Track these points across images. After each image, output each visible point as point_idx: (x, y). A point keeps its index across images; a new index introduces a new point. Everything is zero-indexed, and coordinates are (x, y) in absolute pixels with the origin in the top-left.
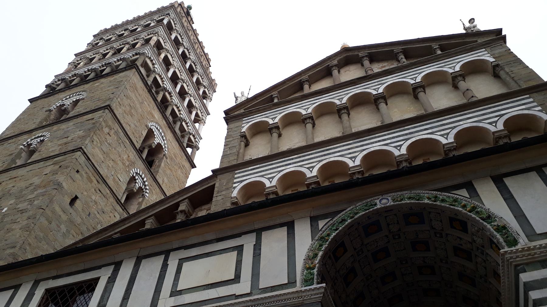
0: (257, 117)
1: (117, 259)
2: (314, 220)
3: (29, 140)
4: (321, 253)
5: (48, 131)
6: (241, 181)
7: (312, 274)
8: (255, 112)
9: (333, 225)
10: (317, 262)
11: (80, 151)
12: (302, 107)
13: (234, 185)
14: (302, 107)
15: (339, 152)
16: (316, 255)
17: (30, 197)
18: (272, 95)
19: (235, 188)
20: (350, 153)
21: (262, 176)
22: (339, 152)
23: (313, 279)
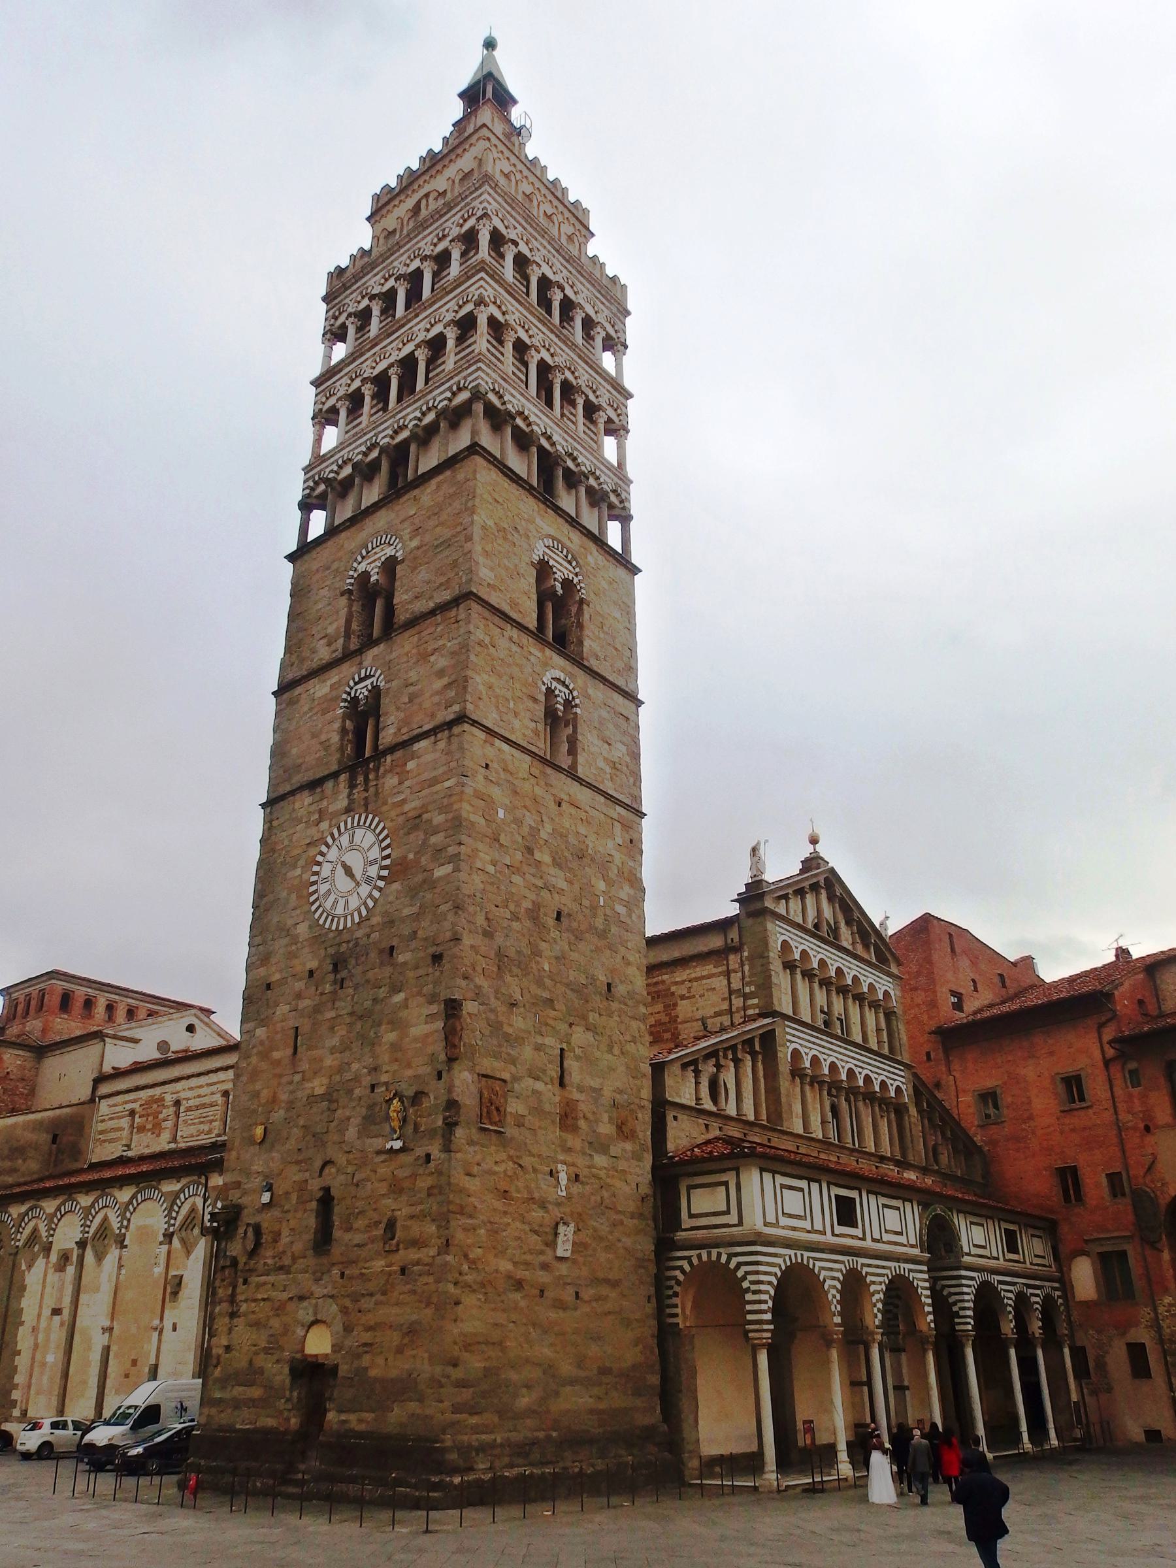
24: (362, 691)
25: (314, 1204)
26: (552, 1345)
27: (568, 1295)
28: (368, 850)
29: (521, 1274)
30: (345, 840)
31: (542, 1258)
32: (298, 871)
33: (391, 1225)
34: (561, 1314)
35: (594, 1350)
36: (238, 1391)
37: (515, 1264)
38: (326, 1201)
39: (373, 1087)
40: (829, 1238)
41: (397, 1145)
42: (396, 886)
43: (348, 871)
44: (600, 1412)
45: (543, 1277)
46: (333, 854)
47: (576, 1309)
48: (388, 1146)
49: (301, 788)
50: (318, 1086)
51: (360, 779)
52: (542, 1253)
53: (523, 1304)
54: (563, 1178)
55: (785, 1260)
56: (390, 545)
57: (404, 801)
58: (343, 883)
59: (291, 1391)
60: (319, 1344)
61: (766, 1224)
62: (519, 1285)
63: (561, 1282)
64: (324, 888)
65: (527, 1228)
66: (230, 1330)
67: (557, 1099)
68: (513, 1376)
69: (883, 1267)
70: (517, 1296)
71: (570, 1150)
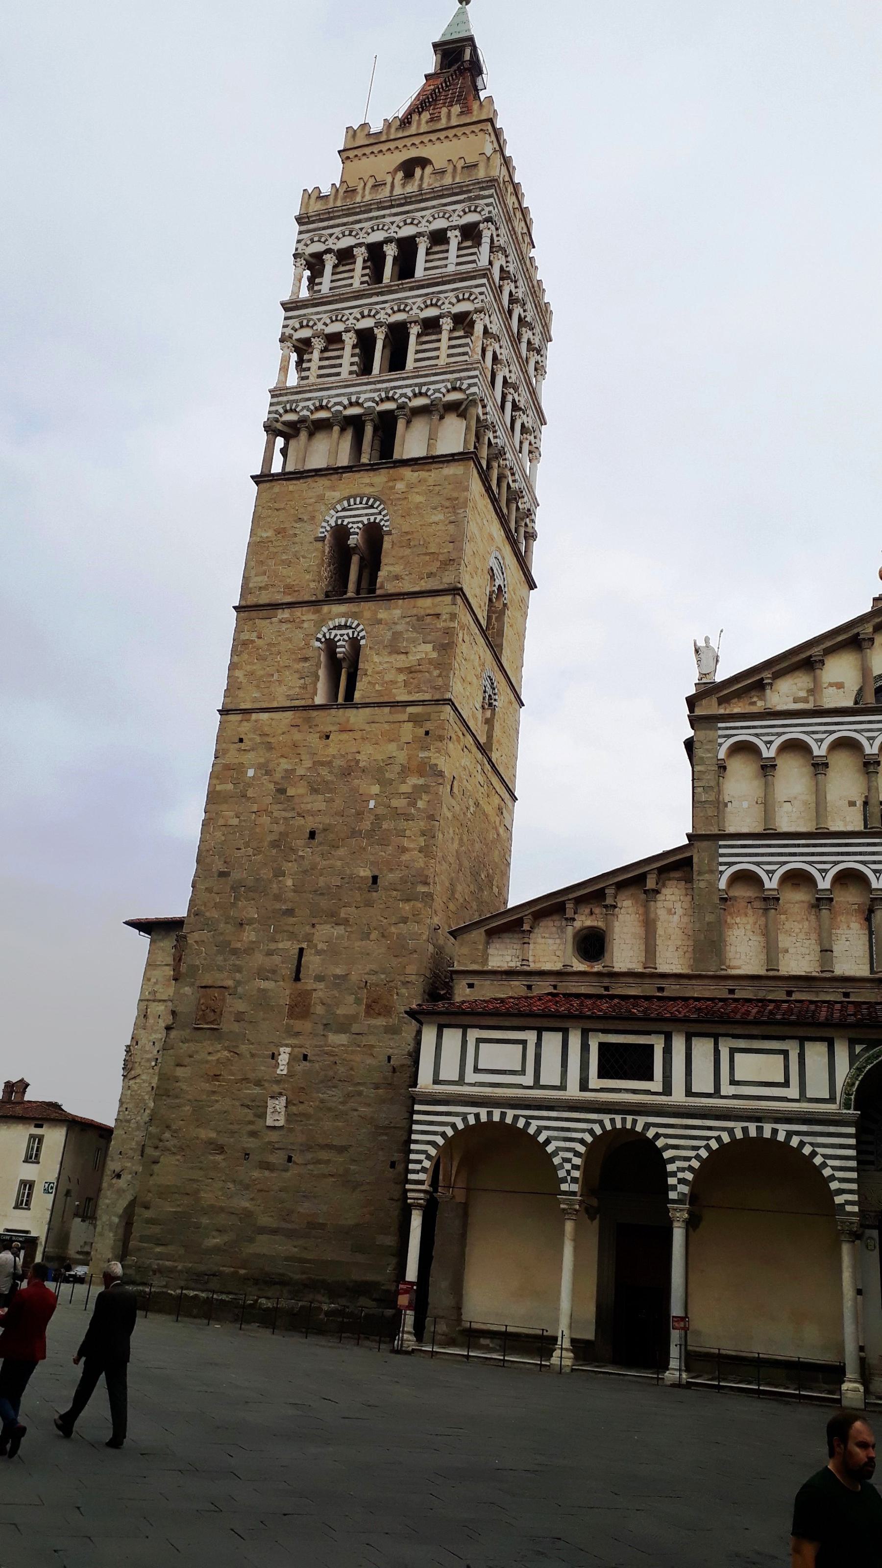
0: (742, 728)
1: (666, 1029)
2: (852, 1043)
3: (325, 629)
4: (857, 1083)
5: (355, 615)
6: (730, 864)
7: (850, 1100)
8: (737, 718)
9: (869, 1058)
10: (854, 1089)
11: (449, 704)
12: (814, 732)
13: (721, 868)
14: (814, 732)
15: (861, 854)
16: (853, 1084)
17: (405, 788)
18: (762, 679)
19: (721, 872)
20: (875, 862)
21: (758, 864)
22: (861, 854)
23: (851, 1104)
26: (252, 1199)
27: (278, 1158)
29: (223, 1140)
31: (251, 1127)
34: (267, 1173)
35: (305, 1207)
37: (219, 1132)
40: (573, 1091)
44: (302, 1261)
45: (250, 1143)
47: (286, 1170)
52: (251, 1123)
53: (223, 1164)
54: (283, 1058)
55: (465, 1120)
61: (436, 1081)
62: (221, 1149)
63: (273, 1148)
65: (237, 1103)
67: (288, 992)
68: (205, 1221)
69: (710, 1128)
70: (219, 1158)
71: (298, 1034)
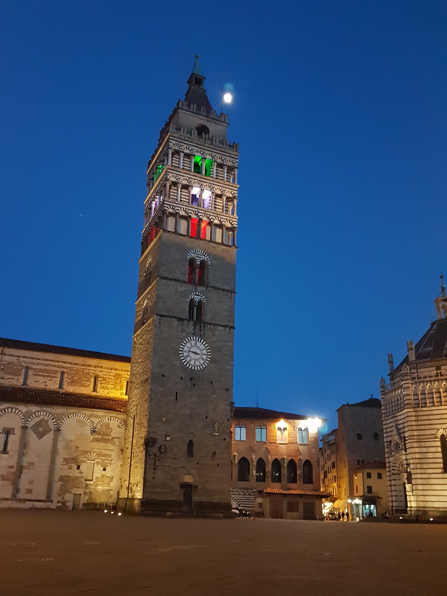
24: (197, 299)
25: (187, 443)
28: (203, 350)
30: (193, 343)
32: (174, 344)
33: (214, 453)
36: (159, 490)
38: (191, 444)
39: (206, 418)
41: (217, 434)
42: (212, 365)
43: (195, 353)
46: (188, 345)
48: (214, 434)
49: (175, 317)
50: (187, 412)
51: (198, 327)
56: (204, 256)
57: (214, 341)
58: (192, 355)
59: (180, 491)
60: (188, 479)
64: (185, 354)
66: (154, 473)
